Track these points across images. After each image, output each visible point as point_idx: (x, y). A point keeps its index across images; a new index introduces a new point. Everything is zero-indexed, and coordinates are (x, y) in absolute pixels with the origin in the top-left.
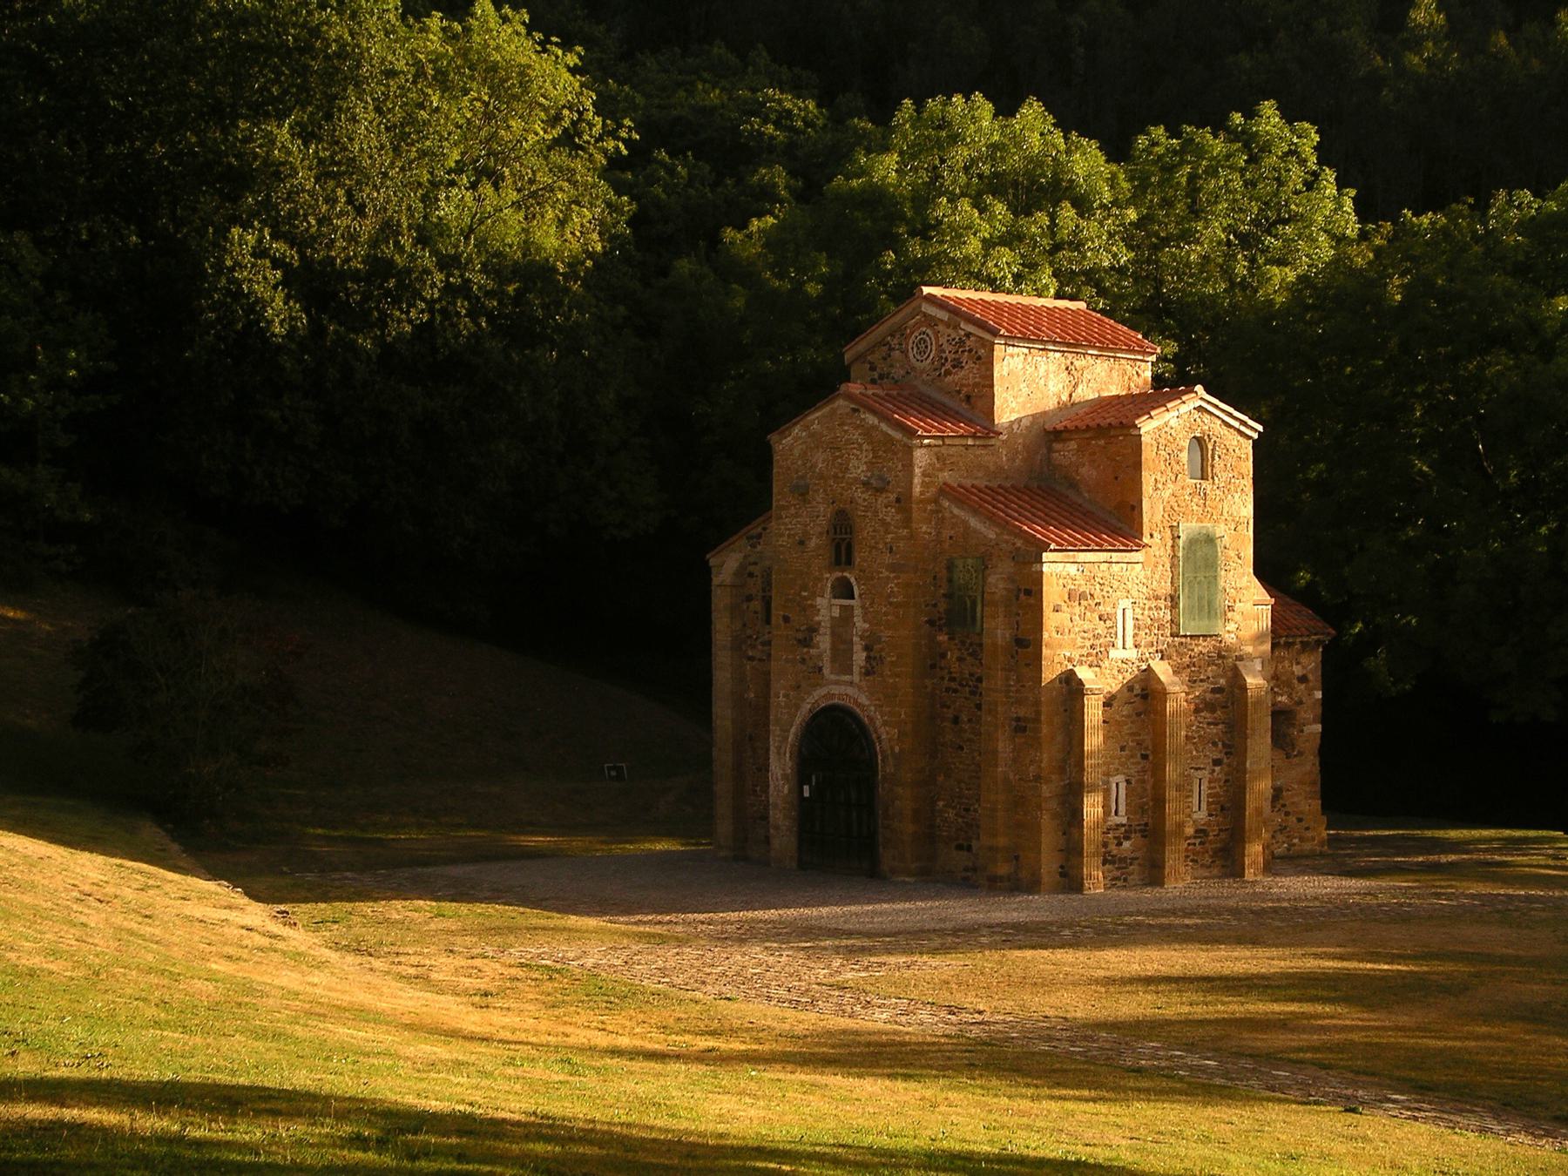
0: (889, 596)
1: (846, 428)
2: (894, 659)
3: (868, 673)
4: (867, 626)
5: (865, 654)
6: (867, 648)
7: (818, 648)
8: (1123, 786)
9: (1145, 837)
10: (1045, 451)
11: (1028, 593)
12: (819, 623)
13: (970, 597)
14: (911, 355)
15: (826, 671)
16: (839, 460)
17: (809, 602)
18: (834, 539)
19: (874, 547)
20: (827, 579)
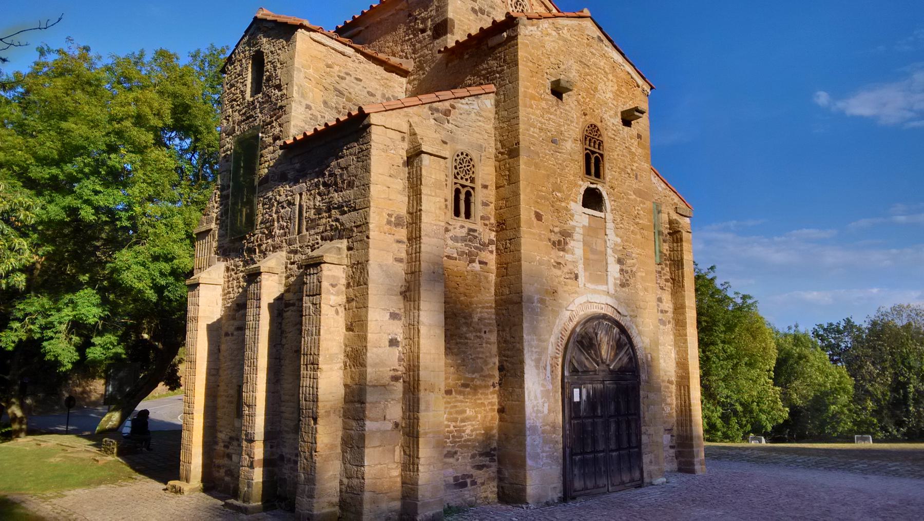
1: (594, 51)
2: (644, 274)
3: (623, 285)
4: (619, 240)
6: (620, 261)
7: (573, 254)
12: (574, 227)
15: (581, 279)
16: (589, 77)
17: (563, 204)
18: (586, 149)
19: (623, 170)
20: (581, 186)
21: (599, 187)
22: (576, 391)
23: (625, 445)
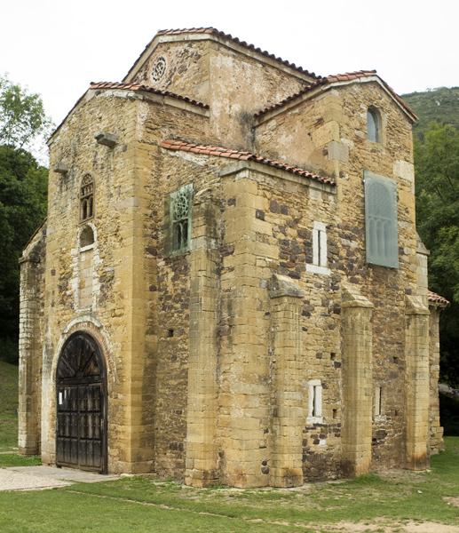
0: (118, 230)
2: (119, 283)
3: (100, 301)
5: (100, 285)
6: (102, 279)
8: (319, 389)
9: (337, 436)
10: (249, 134)
11: (232, 202)
13: (182, 222)
14: (151, 79)
21: (89, 224)
22: (61, 394)
23: (90, 436)
